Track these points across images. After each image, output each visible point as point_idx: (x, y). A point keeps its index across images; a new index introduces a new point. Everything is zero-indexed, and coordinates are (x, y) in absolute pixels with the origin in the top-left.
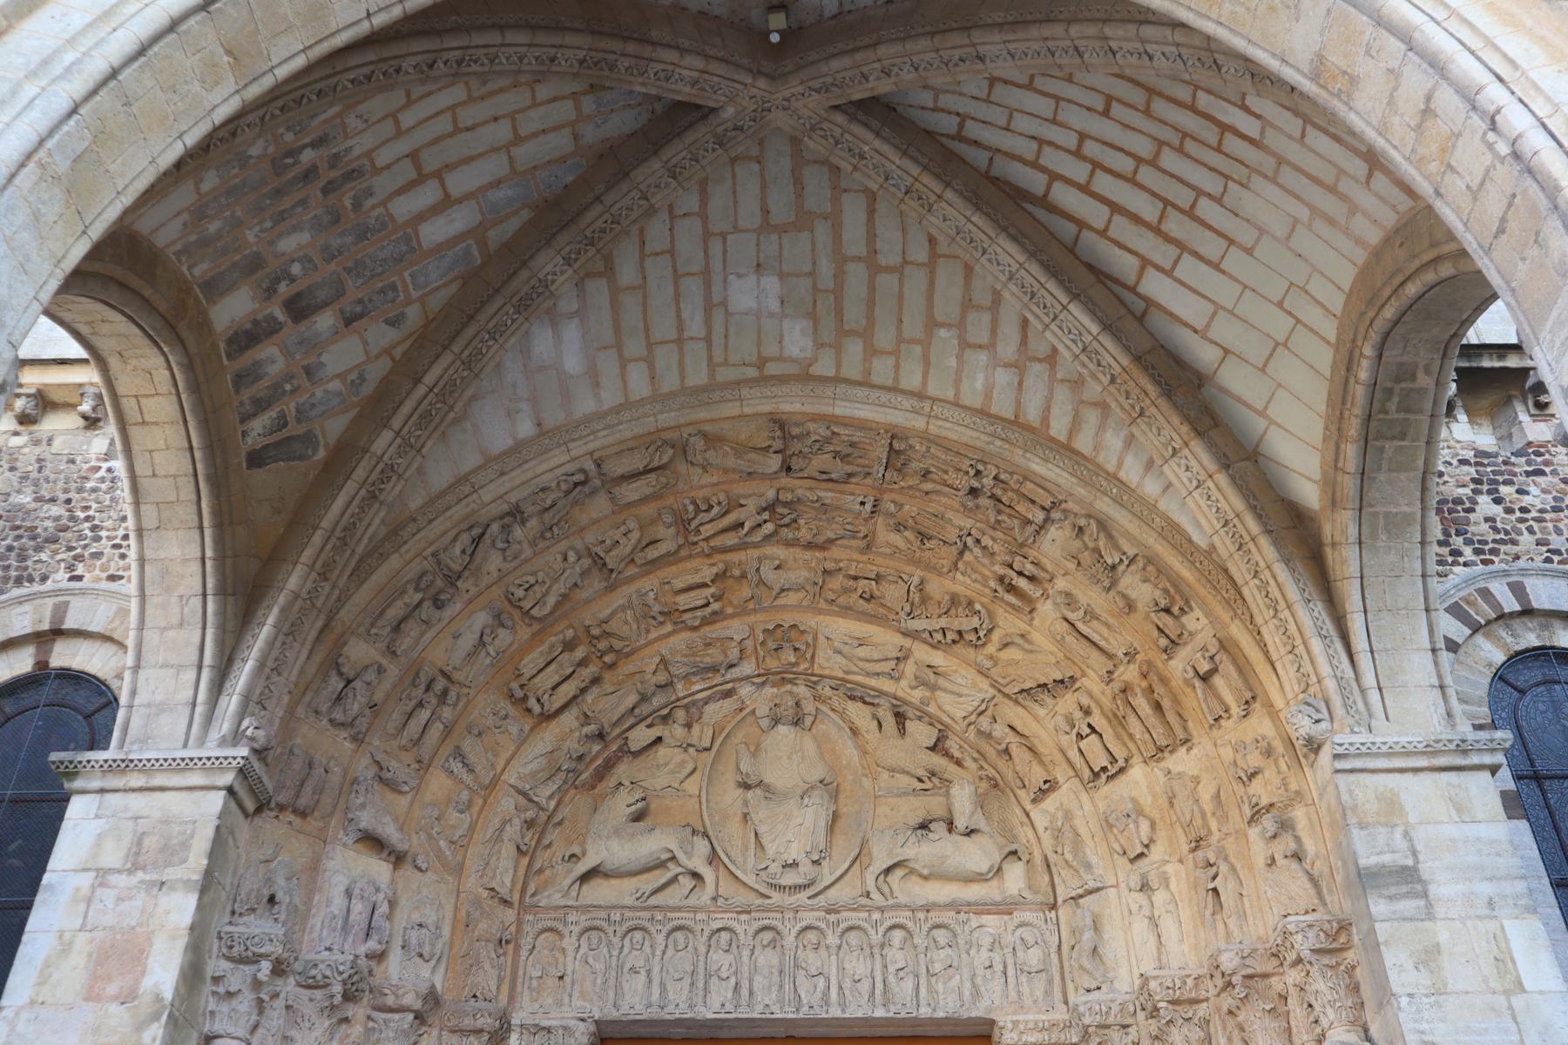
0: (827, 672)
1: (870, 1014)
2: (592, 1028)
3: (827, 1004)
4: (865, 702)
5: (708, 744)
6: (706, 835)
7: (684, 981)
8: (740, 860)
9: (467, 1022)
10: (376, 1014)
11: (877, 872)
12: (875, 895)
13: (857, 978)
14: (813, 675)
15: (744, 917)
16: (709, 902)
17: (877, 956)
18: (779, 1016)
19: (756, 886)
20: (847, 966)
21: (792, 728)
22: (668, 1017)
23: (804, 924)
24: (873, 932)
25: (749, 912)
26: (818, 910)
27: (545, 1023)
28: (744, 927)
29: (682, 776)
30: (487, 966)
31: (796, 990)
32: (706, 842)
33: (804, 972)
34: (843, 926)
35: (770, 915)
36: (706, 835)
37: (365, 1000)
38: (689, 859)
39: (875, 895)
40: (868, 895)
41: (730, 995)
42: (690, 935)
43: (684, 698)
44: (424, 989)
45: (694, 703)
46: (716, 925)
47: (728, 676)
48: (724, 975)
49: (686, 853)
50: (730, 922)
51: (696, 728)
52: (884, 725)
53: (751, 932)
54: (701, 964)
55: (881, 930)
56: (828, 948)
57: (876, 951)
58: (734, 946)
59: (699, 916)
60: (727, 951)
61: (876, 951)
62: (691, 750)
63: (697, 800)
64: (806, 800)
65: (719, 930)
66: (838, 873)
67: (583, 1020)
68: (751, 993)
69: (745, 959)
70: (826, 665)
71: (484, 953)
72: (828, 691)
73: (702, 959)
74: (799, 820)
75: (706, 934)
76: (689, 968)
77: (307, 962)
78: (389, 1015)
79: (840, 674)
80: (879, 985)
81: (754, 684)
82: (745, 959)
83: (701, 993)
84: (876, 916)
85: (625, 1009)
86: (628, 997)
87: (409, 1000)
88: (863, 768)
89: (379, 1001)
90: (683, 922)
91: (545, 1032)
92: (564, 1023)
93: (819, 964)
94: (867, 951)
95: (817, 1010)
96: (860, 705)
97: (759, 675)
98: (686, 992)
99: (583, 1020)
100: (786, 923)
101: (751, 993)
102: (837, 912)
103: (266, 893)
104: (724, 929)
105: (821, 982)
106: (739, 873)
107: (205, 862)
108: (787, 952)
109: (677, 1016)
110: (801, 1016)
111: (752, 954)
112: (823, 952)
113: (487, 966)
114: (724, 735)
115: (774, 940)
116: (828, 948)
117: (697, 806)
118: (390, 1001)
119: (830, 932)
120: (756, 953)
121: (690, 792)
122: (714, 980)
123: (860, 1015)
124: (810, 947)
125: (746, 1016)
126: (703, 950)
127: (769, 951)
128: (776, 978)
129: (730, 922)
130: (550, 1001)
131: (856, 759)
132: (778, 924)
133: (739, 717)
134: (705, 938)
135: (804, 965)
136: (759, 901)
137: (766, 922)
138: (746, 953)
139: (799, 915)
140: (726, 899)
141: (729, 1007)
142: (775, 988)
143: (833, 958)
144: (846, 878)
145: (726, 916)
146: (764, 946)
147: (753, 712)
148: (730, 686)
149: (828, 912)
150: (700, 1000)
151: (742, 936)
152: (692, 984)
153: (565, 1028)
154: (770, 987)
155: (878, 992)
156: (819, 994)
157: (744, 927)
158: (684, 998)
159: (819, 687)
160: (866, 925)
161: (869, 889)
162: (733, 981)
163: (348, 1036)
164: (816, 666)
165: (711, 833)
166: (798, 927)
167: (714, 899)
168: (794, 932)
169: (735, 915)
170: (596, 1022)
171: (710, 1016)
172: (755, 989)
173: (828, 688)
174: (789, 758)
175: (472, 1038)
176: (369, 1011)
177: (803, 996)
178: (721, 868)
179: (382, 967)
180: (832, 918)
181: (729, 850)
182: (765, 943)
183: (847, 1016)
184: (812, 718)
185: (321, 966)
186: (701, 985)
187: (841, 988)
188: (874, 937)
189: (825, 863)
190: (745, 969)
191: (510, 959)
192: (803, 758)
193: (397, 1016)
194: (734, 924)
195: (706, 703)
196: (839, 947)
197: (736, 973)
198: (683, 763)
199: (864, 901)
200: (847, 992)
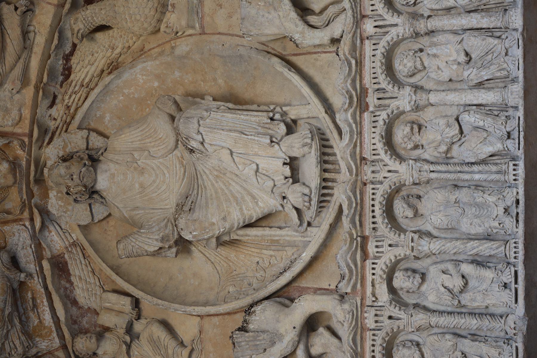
0: (27, 113)
1: (518, 35)
3: (504, 107)
4: (72, 53)
5: (125, 303)
6: (249, 310)
7: (467, 350)
8: (290, 252)
11: (301, 26)
12: (336, 28)
13: (462, 58)
14: (31, 135)
15: (371, 248)
16: (346, 306)
17: (432, 24)
18: (521, 190)
19: (325, 227)
20: (445, 75)
21: (102, 167)
23: (380, 146)
24: (393, 31)
25: (365, 239)
26: (360, 124)
28: (386, 248)
29: (172, 344)
31: (483, 162)
32: (258, 309)
33: (455, 147)
34: (384, 82)
35: (368, 202)
36: (249, 310)
38: (280, 337)
39: (336, 28)
40: (335, 41)
41: (489, 274)
42: (401, 338)
43: (62, 337)
45: (72, 321)
46: (384, 296)
47: (32, 267)
48: (458, 283)
49: (273, 343)
50: (378, 271)
51: (106, 319)
52: (99, 21)
53: (392, 237)
54: (443, 320)
55: (390, 18)
56: (417, 108)
57: (422, 26)
58: (417, 265)
59: (370, 323)
60: (423, 277)
61: (422, 26)
62: (138, 327)
63: (206, 319)
64: (194, 144)
65: (392, 290)
66: (306, 90)
68: (488, 237)
69: (435, 246)
70: (15, 114)
72: (58, 111)
73: (434, 319)
74: (225, 155)
75: (396, 312)
76: (448, 341)
79: (29, 92)
80: (475, 20)
81: (43, 226)
82: (435, 246)
83: (486, 323)
84: (369, 27)
88: (161, 54)
90: (378, 349)
93: (442, 122)
94: (425, 41)
95: (512, 125)
96: (74, 60)
97: (32, 220)
100: (379, 177)
101: (488, 237)
102: (364, 92)
104: (390, 280)
105: (468, 119)
106: (307, 256)
108: (425, 176)
110: (520, 153)
111: (429, 234)
112: (427, 115)
114: (115, 277)
115: (406, 199)
116: (417, 108)
117: (216, 320)
119: (394, 104)
120: (429, 228)
121: (196, 331)
122: (466, 299)
123: (519, 53)
124: (417, 138)
125: (521, 246)
126: (420, 318)
127: (424, 207)
128: (463, 195)
129: (378, 271)
131: (150, 65)
132: (382, 190)
133: (90, 251)
134: (402, 315)
135: (443, 148)
136: (345, 221)
137: (378, 211)
138: (425, 246)
139: (367, 155)
140: (343, 277)
141: (507, 277)
142: (479, 197)
143: (433, 98)
144: (318, 78)
145: (369, 278)
146: (416, 214)
147: (85, 229)
148: (46, 264)
149: (363, 107)
150: (498, 325)
151: (400, 252)
152: (474, 336)
154: (477, 205)
155: (485, 22)
156: (487, 123)
157: (386, 248)
159: (52, 125)
160: (383, 43)
161: (326, 40)
162: (467, 269)
164: (18, 130)
165: (248, 300)
166: (386, 157)
167: (342, 297)
168: (394, 165)
169: (368, 263)
171: (520, 309)
172: (480, 230)
173: (54, 112)
174: (142, 171)
177: (489, 149)
178: (303, 283)
180: (372, 100)
181: (276, 270)
182: (410, 213)
183: (520, 74)
184: (93, 135)
186: (473, 323)
187: (480, 85)
188: (400, 30)
189: (293, 114)
190: (449, 246)
192: (142, 150)
194: (382, 265)
195: (75, 302)
196: (417, 88)
197: (457, 262)
198: (154, 343)
199: (345, 47)
200: (485, 75)
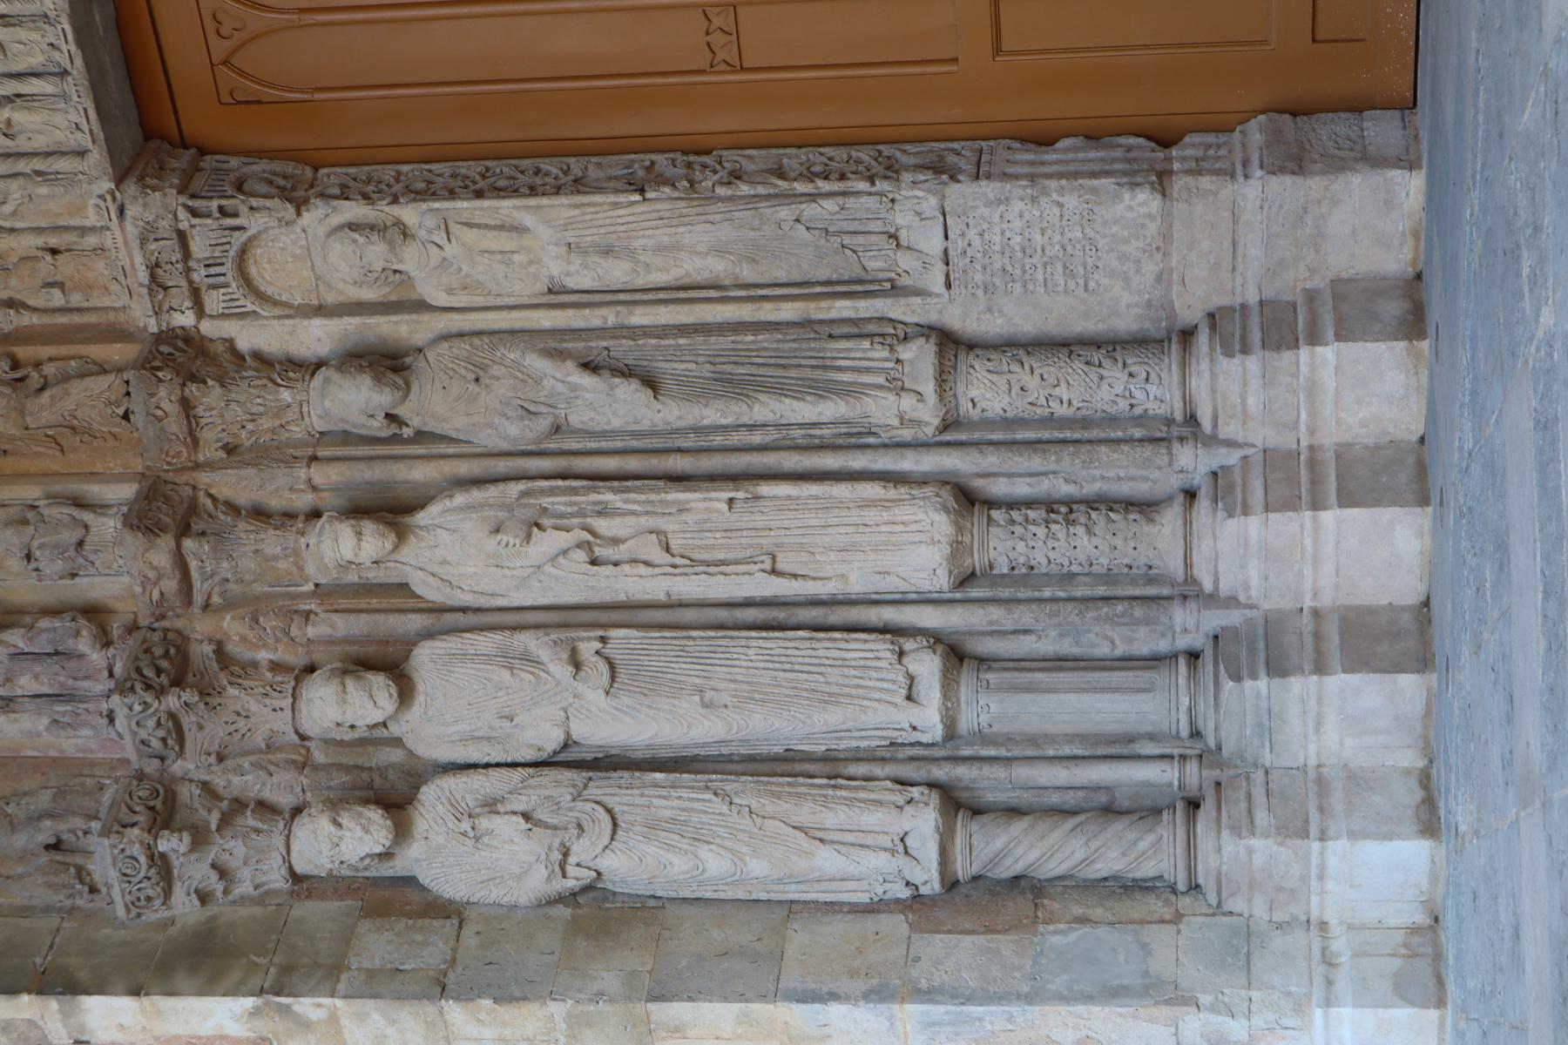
2: (131, 188)
9: (175, 426)
10: (198, 599)
22: (79, 61)
27: (143, 275)
30: (69, 404)
37: (179, 624)
44: (135, 541)
67: (121, 211)
71: (46, 417)
77: (140, 755)
78: (194, 574)
85: (85, 140)
86: (60, 136)
87: (161, 556)
89: (176, 601)
91: (159, 271)
92: (135, 244)
98: (22, 33)
99: (121, 211)
103: (45, 858)
107: (25, 998)
109: (73, 47)
113: (69, 404)
118: (171, 585)
130: (100, 265)
153: (143, 241)
158: (35, 36)
163: (244, 639)
170: (119, 180)
175: (200, 410)
176: (196, 609)
179: (119, 606)
185: (143, 734)
191: (46, 351)
193: (193, 565)
